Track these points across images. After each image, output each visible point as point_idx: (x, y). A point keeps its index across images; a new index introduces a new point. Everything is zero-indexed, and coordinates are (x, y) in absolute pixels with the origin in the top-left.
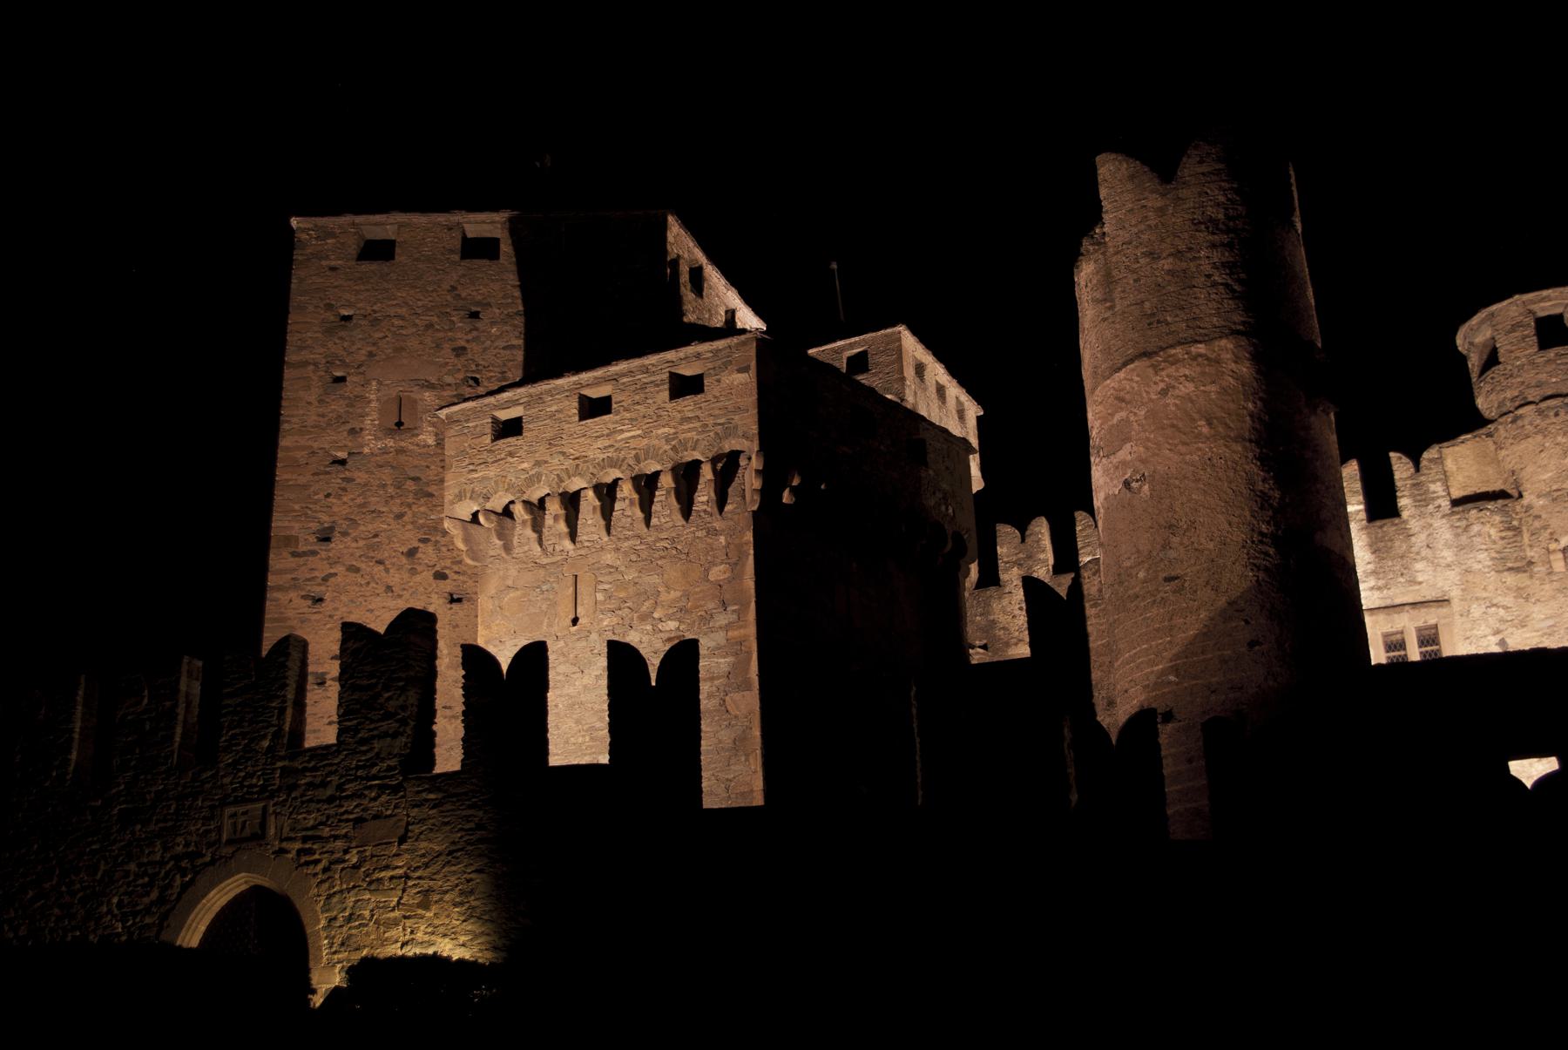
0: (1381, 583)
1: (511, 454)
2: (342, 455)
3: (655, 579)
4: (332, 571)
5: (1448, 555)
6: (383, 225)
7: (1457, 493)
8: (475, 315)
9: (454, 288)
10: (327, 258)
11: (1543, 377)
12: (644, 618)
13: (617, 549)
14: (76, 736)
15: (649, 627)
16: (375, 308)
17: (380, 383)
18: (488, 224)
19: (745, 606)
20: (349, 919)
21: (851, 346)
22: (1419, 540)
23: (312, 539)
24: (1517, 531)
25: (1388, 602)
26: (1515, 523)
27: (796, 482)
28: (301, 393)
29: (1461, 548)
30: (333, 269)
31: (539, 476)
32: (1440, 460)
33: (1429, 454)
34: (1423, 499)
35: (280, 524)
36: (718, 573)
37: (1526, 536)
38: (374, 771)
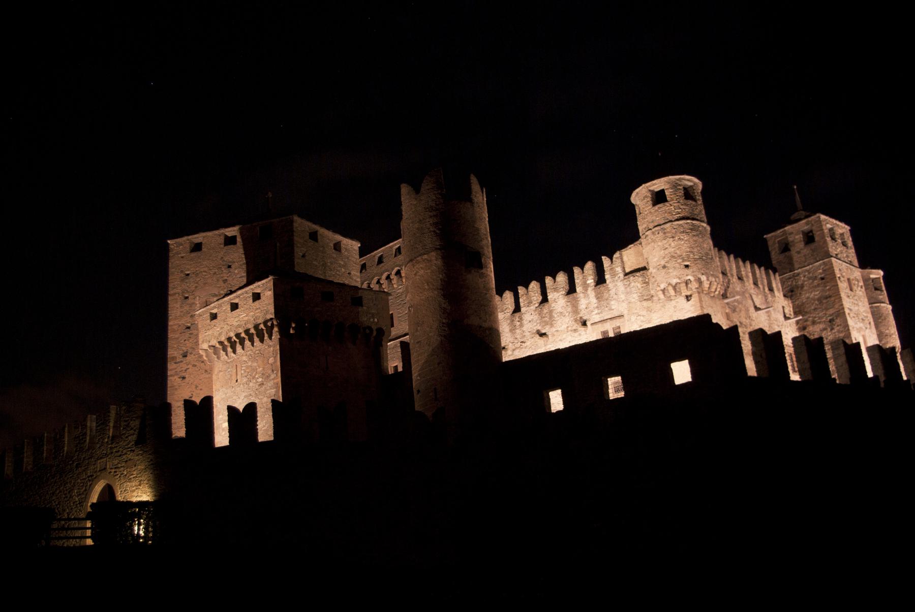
0: (599, 311)
1: (215, 326)
2: (189, 325)
3: (255, 364)
4: (188, 367)
5: (623, 297)
6: (198, 238)
7: (628, 270)
8: (230, 267)
9: (222, 258)
10: (180, 254)
11: (654, 218)
12: (254, 378)
13: (246, 355)
14: (66, 442)
15: (255, 381)
16: (197, 269)
17: (199, 297)
18: (232, 231)
19: (278, 371)
20: (125, 491)
21: (395, 244)
22: (612, 292)
23: (181, 357)
24: (647, 283)
25: (602, 319)
26: (647, 280)
27: (293, 325)
28: (175, 305)
29: (627, 293)
30: (182, 257)
31: (222, 332)
32: (621, 258)
33: (617, 255)
34: (614, 275)
35: (170, 353)
36: (271, 360)
37: (651, 285)
38: (129, 446)
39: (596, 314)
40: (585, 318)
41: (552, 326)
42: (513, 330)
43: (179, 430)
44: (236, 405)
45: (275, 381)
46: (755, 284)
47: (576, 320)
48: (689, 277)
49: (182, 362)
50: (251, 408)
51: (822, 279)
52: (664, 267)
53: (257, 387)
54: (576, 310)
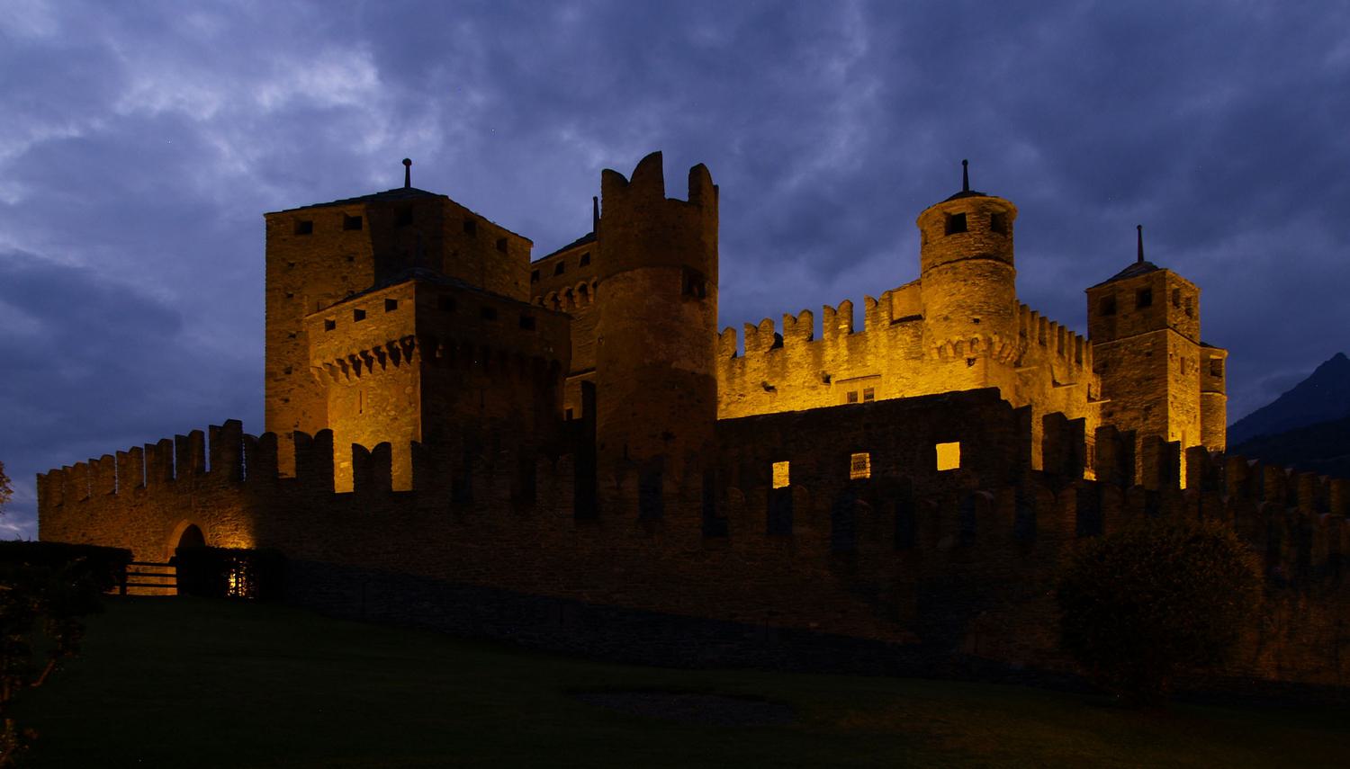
0: (850, 367)
1: (332, 338)
2: (294, 332)
3: (387, 393)
5: (883, 351)
7: (896, 317)
12: (384, 410)
13: (375, 380)
15: (385, 414)
21: (583, 250)
23: (283, 373)
24: (920, 337)
25: (852, 377)
26: (920, 333)
27: (440, 347)
29: (891, 347)
31: (341, 348)
36: (409, 390)
37: (924, 340)
38: (221, 482)
39: (845, 369)
40: (829, 373)
41: (783, 378)
42: (730, 379)
43: (288, 467)
44: (366, 445)
45: (413, 416)
46: (1060, 352)
47: (816, 375)
48: (976, 336)
49: (283, 379)
50: (384, 449)
51: (1149, 354)
52: (946, 318)
53: (388, 421)
54: (818, 360)
